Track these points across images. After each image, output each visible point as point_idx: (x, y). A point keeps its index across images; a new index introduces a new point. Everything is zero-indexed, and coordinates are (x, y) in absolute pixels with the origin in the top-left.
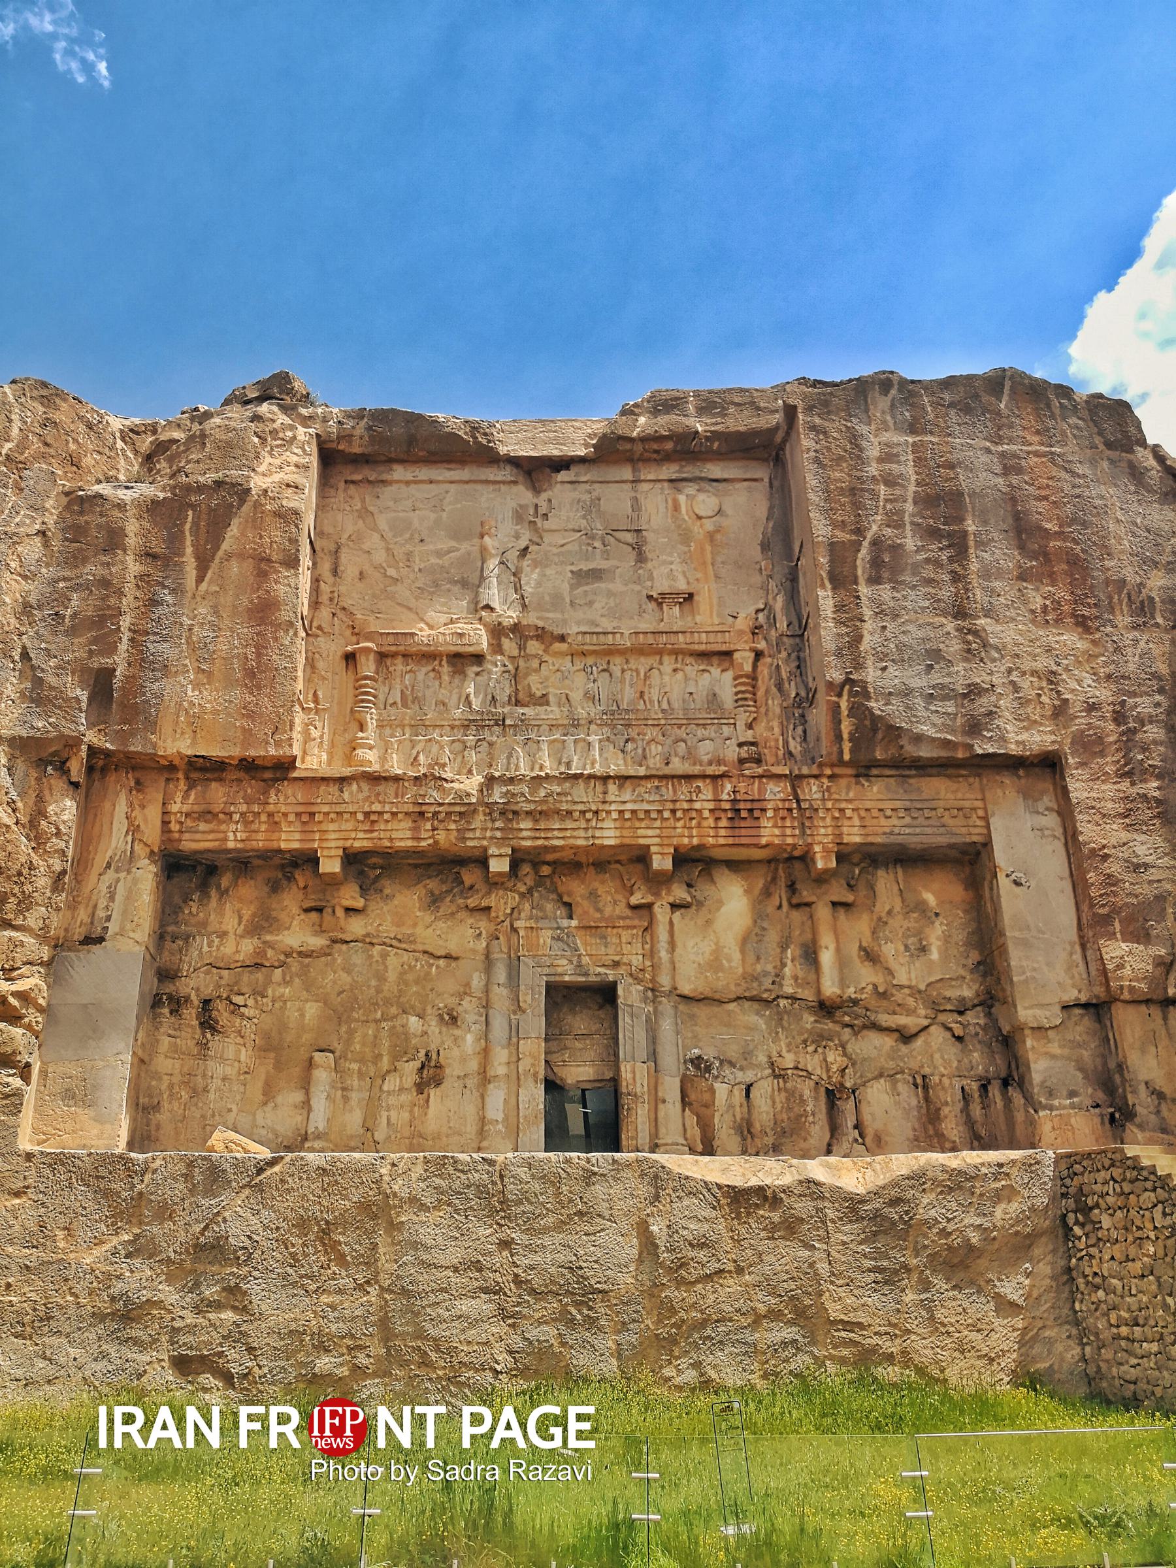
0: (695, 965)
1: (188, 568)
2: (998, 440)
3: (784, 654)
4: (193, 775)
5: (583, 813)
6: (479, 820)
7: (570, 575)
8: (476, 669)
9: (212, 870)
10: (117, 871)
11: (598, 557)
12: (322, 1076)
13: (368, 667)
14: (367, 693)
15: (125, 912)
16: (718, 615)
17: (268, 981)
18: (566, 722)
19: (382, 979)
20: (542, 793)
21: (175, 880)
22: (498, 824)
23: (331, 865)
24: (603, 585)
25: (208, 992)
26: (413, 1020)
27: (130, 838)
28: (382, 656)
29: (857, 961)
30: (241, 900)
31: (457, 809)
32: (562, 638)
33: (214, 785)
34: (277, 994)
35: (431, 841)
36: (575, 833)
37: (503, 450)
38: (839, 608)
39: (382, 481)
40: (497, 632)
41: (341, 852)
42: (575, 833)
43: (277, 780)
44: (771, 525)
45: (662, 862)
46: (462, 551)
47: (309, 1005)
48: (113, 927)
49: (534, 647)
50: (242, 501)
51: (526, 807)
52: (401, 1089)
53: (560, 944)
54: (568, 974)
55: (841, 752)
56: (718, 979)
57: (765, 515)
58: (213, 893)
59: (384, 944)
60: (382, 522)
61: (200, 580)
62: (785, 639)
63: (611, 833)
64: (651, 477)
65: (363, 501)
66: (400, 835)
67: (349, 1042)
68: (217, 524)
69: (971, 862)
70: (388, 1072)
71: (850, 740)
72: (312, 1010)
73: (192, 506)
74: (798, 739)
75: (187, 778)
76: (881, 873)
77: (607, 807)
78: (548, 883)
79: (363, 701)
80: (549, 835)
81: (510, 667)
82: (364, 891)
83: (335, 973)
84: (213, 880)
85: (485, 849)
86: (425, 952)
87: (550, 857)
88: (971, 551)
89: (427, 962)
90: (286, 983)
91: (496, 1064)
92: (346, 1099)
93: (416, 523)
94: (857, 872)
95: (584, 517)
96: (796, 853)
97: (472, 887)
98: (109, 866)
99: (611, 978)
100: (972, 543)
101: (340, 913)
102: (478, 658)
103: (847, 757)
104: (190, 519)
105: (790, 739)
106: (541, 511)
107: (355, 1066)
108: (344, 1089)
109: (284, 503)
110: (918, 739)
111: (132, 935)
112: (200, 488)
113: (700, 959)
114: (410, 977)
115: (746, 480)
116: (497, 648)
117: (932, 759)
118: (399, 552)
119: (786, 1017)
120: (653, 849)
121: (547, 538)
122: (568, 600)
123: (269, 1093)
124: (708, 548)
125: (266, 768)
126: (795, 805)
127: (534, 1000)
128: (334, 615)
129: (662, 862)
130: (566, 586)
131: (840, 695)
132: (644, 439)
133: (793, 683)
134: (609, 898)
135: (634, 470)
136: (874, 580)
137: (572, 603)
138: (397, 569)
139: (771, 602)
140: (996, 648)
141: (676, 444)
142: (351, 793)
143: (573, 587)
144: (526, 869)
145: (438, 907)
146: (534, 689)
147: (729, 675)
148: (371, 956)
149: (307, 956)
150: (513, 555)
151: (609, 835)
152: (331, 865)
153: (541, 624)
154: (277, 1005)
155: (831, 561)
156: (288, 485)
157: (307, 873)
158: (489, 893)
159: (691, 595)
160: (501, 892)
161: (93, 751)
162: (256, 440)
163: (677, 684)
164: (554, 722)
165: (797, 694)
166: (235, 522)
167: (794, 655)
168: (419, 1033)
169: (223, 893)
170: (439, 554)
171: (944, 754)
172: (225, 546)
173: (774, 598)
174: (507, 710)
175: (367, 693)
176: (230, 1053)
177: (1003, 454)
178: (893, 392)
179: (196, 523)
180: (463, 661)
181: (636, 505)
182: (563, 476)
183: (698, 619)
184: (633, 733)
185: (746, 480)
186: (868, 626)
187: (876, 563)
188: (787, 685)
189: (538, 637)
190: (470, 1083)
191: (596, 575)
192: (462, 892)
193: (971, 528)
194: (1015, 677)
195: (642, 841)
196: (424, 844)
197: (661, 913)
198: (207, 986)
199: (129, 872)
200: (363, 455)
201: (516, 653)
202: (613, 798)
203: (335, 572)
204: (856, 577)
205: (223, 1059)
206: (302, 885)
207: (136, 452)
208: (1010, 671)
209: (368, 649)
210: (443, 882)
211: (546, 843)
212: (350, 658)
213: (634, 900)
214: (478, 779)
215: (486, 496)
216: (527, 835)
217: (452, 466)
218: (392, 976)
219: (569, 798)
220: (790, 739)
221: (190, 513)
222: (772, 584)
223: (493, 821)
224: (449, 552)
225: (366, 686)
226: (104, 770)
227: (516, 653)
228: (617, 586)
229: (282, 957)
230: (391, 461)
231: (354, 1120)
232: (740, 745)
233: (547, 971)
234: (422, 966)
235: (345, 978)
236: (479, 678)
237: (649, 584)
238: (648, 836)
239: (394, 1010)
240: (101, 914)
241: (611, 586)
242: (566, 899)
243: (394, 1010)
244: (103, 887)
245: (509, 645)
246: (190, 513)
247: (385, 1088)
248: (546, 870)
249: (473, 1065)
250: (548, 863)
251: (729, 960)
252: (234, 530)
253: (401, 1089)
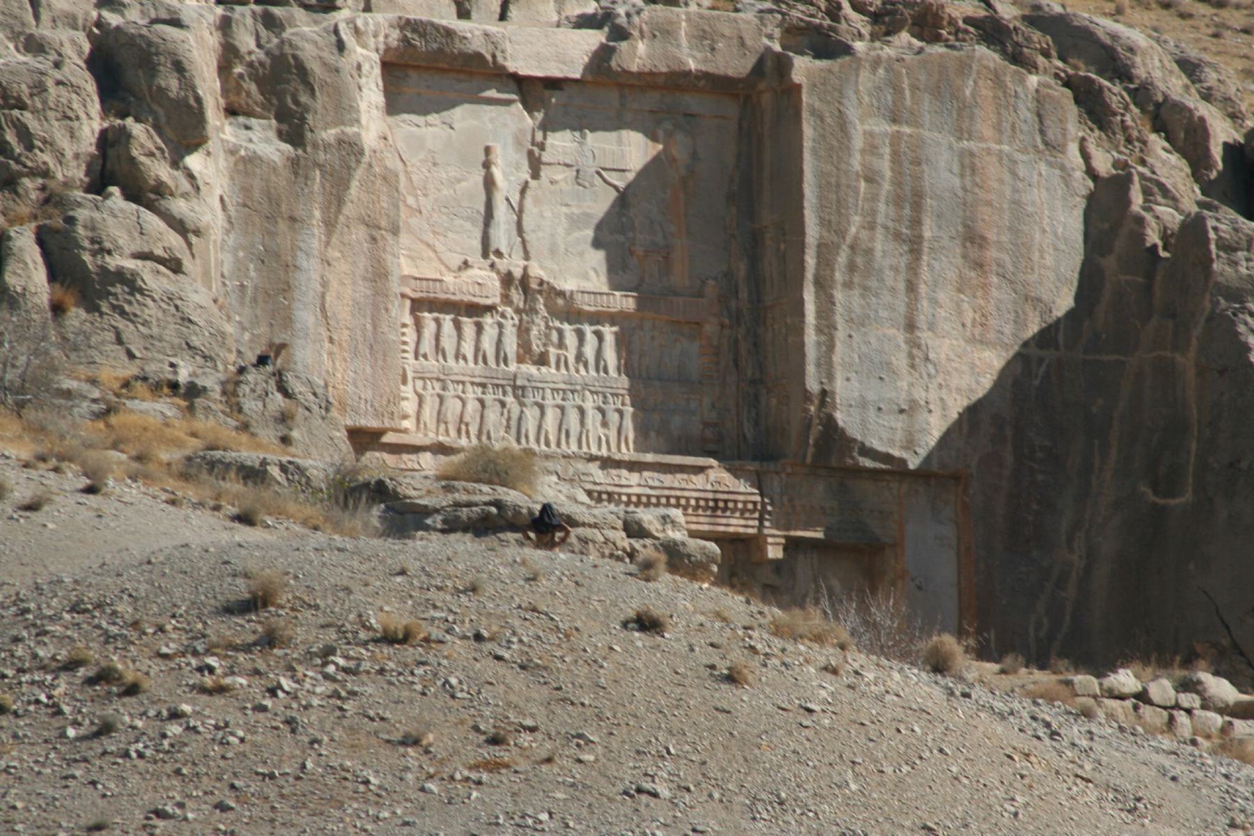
38: (820, 314)
55: (805, 456)
76: (801, 557)
88: (925, 258)
103: (809, 460)
116: (506, 299)
130: (560, 230)
136: (848, 285)
146: (534, 347)
147: (695, 347)
155: (818, 264)
186: (840, 335)
187: (852, 267)
219: (591, 479)
227: (521, 305)
232: (706, 424)
237: (631, 235)
245: (517, 296)
246: (318, 172)
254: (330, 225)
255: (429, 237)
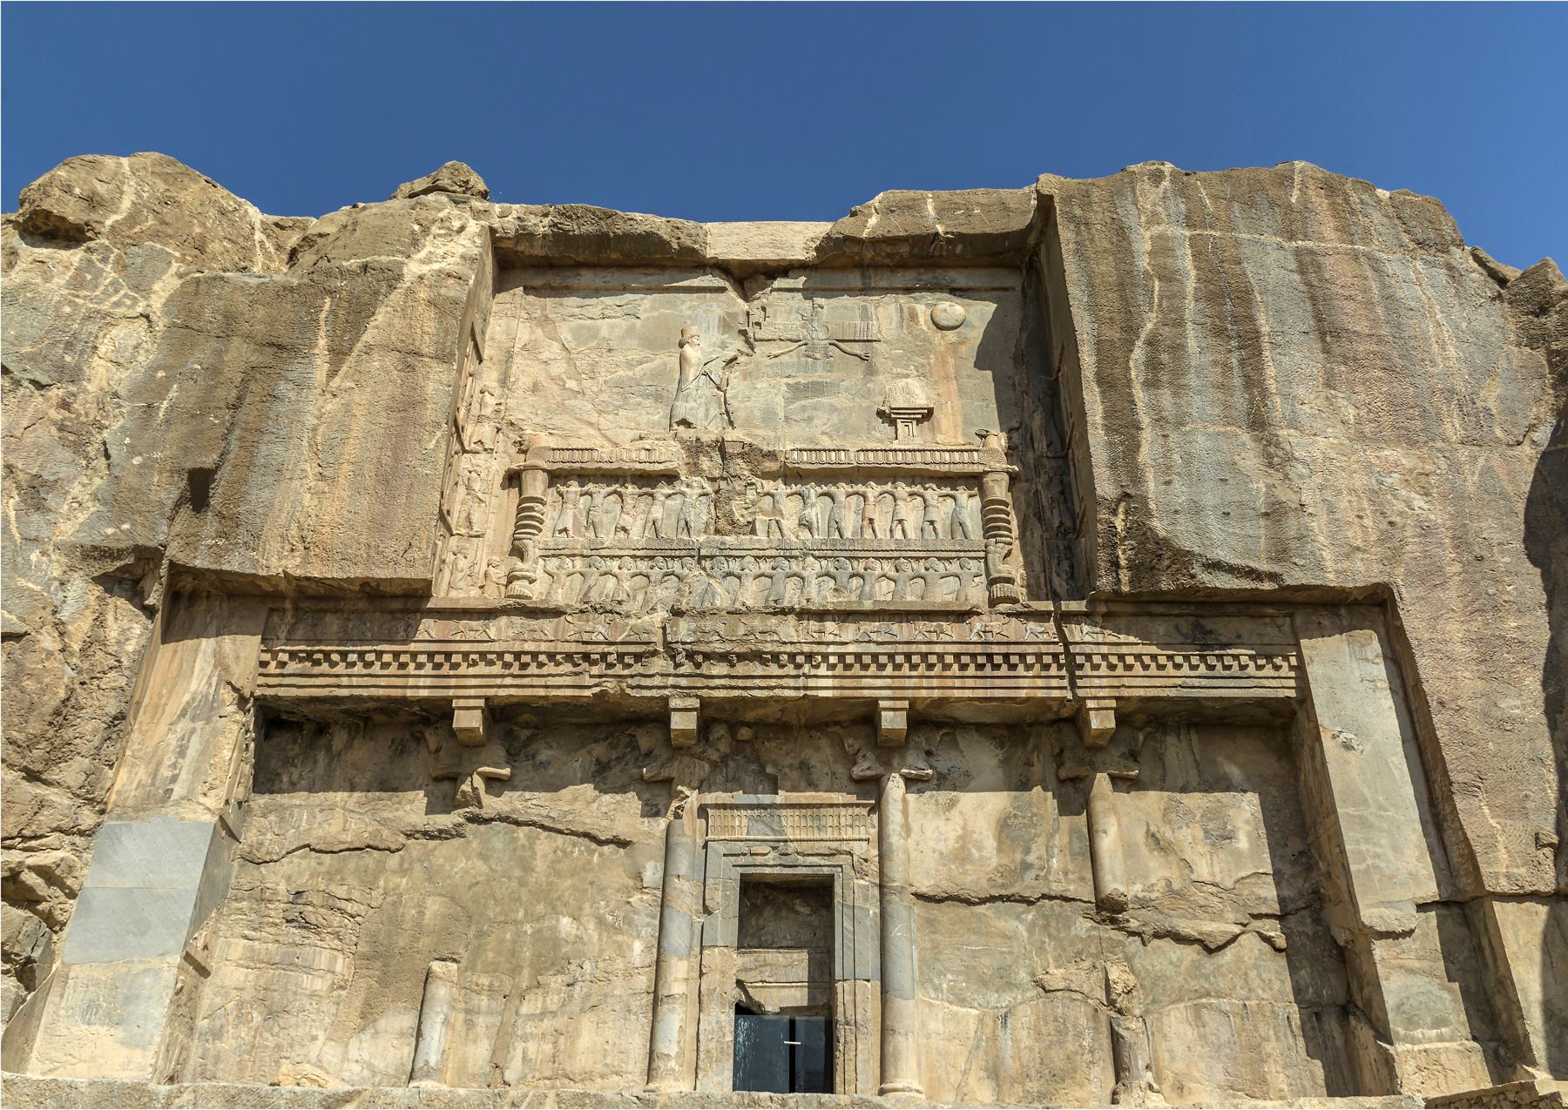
0: (936, 855)
1: (319, 362)
2: (1292, 237)
3: (1044, 478)
4: (304, 605)
5: (792, 656)
6: (660, 664)
7: (785, 388)
8: (667, 490)
9: (322, 729)
10: (193, 720)
11: (820, 369)
12: (441, 992)
13: (536, 485)
14: (532, 518)
15: (196, 772)
16: (964, 435)
17: (381, 869)
18: (774, 553)
19: (527, 868)
20: (741, 631)
21: (275, 741)
22: (682, 670)
23: (469, 720)
24: (825, 400)
25: (302, 882)
26: (565, 922)
27: (214, 680)
28: (556, 477)
29: (1144, 851)
30: (354, 766)
31: (632, 649)
32: (772, 455)
33: (329, 618)
34: (391, 885)
35: (597, 690)
36: (783, 682)
37: (710, 253)
38: (1109, 415)
39: (567, 288)
40: (695, 449)
41: (481, 703)
42: (783, 682)
43: (406, 611)
44: (1025, 335)
45: (893, 720)
46: (658, 362)
47: (429, 901)
48: (179, 790)
49: (740, 467)
50: (392, 288)
51: (719, 647)
52: (544, 1014)
53: (761, 826)
54: (769, 865)
56: (965, 873)
57: (1018, 325)
58: (321, 757)
59: (534, 824)
60: (565, 333)
61: (332, 374)
62: (1045, 461)
63: (829, 682)
64: (883, 284)
65: (544, 308)
66: (560, 683)
67: (478, 950)
68: (357, 314)
69: (1279, 739)
70: (529, 989)
71: (1129, 568)
72: (434, 906)
73: (330, 293)
74: (1064, 576)
75: (296, 609)
76: (1171, 739)
77: (823, 649)
78: (748, 750)
79: (526, 526)
80: (749, 683)
81: (709, 489)
82: (511, 758)
83: (468, 859)
84: (323, 741)
85: (665, 699)
86: (586, 835)
87: (750, 716)
88: (1267, 353)
89: (588, 848)
90: (402, 871)
91: (671, 979)
92: (470, 1024)
93: (604, 332)
94: (1141, 738)
95: (804, 327)
96: (1065, 713)
97: (649, 754)
98: (183, 714)
99: (826, 871)
100: (1266, 345)
101: (478, 782)
102: (671, 477)
104: (327, 307)
105: (1054, 576)
106: (753, 319)
107: (485, 981)
108: (468, 1011)
109: (443, 291)
110: (1215, 566)
111: (202, 799)
112: (343, 273)
113: (941, 847)
114: (563, 866)
115: (994, 289)
116: (695, 469)
117: (1231, 591)
118: (582, 364)
119: (1053, 924)
120: (882, 704)
121: (759, 347)
122: (781, 415)
123: (368, 1015)
124: (951, 361)
125: (394, 597)
126: (1061, 649)
127: (726, 899)
128: (498, 430)
129: (893, 720)
130: (780, 400)
131: (1114, 512)
132: (874, 242)
133: (1056, 512)
134: (826, 770)
135: (863, 277)
137: (787, 418)
138: (579, 381)
139: (1027, 420)
140: (1304, 463)
141: (912, 247)
142: (499, 630)
143: (789, 401)
144: (719, 731)
145: (605, 778)
146: (737, 516)
148: (514, 840)
149: (432, 838)
150: (716, 370)
151: (825, 685)
152: (469, 720)
153: (748, 440)
154: (389, 899)
155: (1099, 362)
156: (449, 275)
157: (440, 732)
158: (671, 759)
159: (930, 412)
160: (686, 760)
161: (176, 570)
162: (416, 227)
163: (908, 515)
164: (761, 553)
165: (1061, 524)
166: (381, 310)
167: (1056, 480)
168: (572, 939)
169: (333, 757)
170: (630, 365)
171: (1246, 584)
172: (368, 337)
173: (1031, 417)
174: (702, 538)
175: (532, 518)
176: (323, 960)
177: (1298, 253)
178: (1166, 184)
179: (332, 312)
180: (647, 479)
181: (865, 315)
182: (779, 283)
183: (939, 438)
184: (859, 567)
185: (994, 289)
187: (1153, 364)
188: (1048, 513)
189: (742, 455)
190: (635, 1004)
191: (817, 389)
192: (637, 760)
193: (1265, 329)
194: (1328, 494)
195: (866, 693)
196: (587, 693)
197: (895, 787)
198: (300, 874)
199: (208, 721)
200: (546, 257)
201: (716, 473)
202: (831, 638)
203: (504, 382)
204: (1129, 381)
205: (309, 969)
206: (433, 746)
207: (279, 248)
208: (1322, 488)
209: (536, 468)
210: (613, 747)
211: (745, 693)
212: (513, 479)
213: (857, 771)
214: (661, 615)
215: (686, 304)
216: (720, 682)
217: (651, 271)
218: (540, 865)
219: (776, 638)
220: (1054, 576)
221: (328, 300)
222: (1028, 401)
223: (677, 666)
224: (641, 363)
225: (531, 509)
226: (194, 596)
228: (841, 401)
229: (402, 839)
230: (578, 266)
231: (480, 1053)
233: (742, 860)
234: (581, 853)
235: (481, 866)
236: (669, 502)
238: (873, 685)
239: (540, 908)
240: (166, 773)
241: (833, 400)
242: (769, 770)
243: (540, 908)
244: (173, 740)
246: (328, 300)
247: (524, 1010)
248: (745, 733)
249: (643, 981)
250: (749, 725)
251: (980, 849)
252: (381, 317)
253: (544, 1014)
254: (338, 354)
255: (594, 418)
